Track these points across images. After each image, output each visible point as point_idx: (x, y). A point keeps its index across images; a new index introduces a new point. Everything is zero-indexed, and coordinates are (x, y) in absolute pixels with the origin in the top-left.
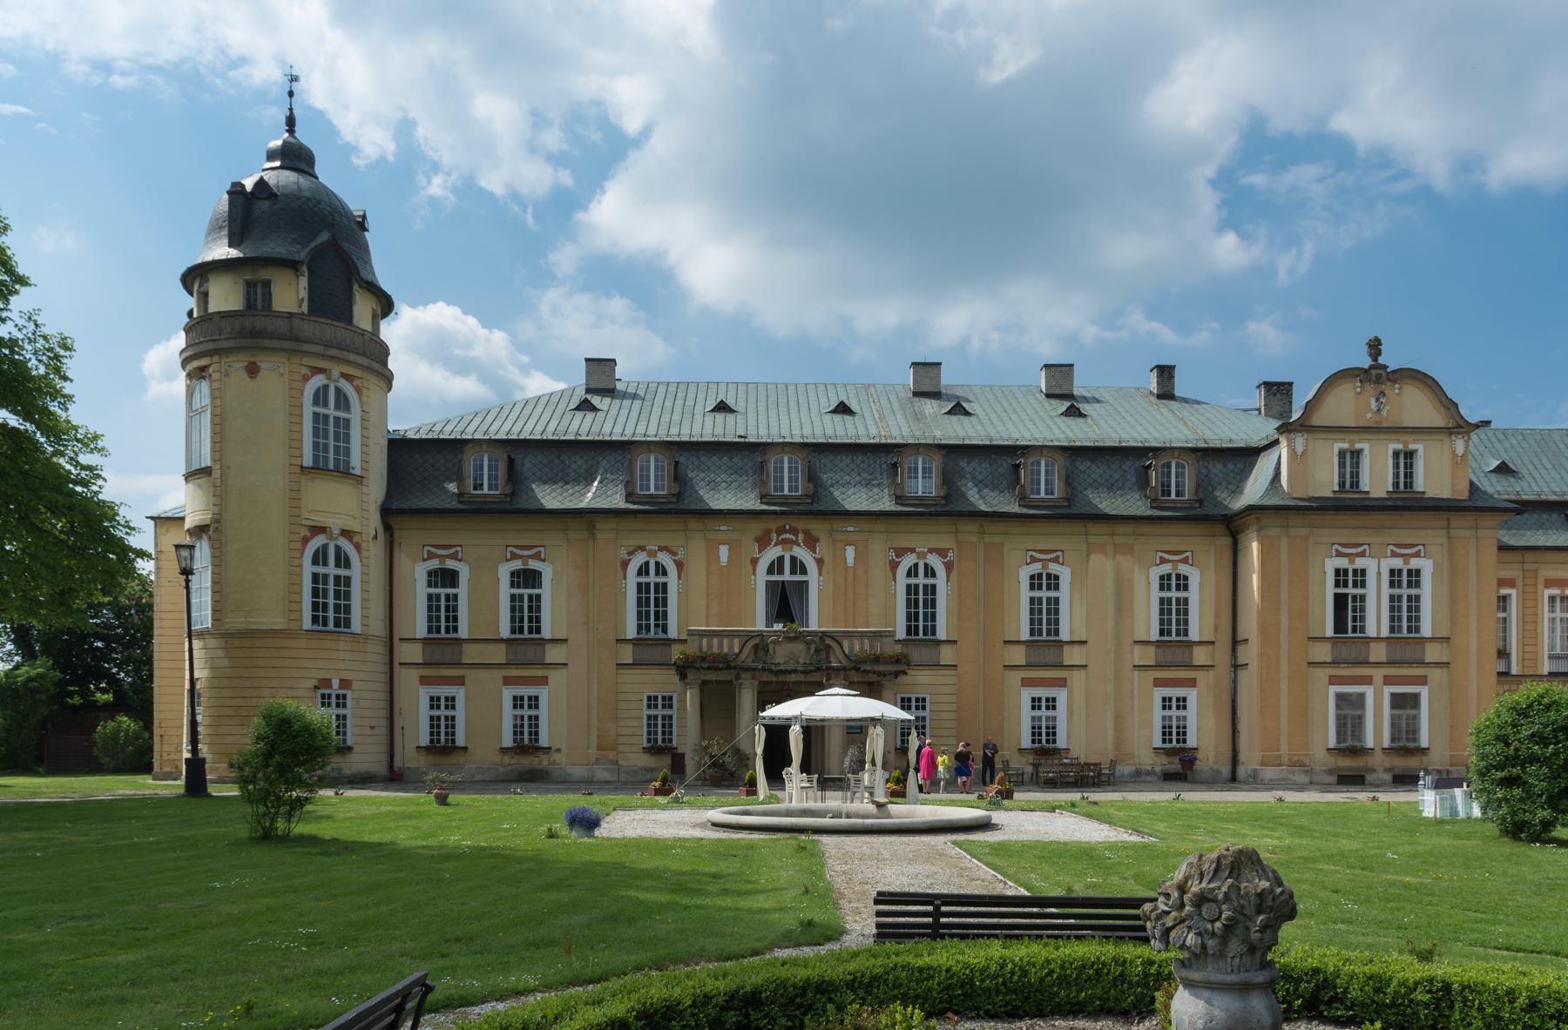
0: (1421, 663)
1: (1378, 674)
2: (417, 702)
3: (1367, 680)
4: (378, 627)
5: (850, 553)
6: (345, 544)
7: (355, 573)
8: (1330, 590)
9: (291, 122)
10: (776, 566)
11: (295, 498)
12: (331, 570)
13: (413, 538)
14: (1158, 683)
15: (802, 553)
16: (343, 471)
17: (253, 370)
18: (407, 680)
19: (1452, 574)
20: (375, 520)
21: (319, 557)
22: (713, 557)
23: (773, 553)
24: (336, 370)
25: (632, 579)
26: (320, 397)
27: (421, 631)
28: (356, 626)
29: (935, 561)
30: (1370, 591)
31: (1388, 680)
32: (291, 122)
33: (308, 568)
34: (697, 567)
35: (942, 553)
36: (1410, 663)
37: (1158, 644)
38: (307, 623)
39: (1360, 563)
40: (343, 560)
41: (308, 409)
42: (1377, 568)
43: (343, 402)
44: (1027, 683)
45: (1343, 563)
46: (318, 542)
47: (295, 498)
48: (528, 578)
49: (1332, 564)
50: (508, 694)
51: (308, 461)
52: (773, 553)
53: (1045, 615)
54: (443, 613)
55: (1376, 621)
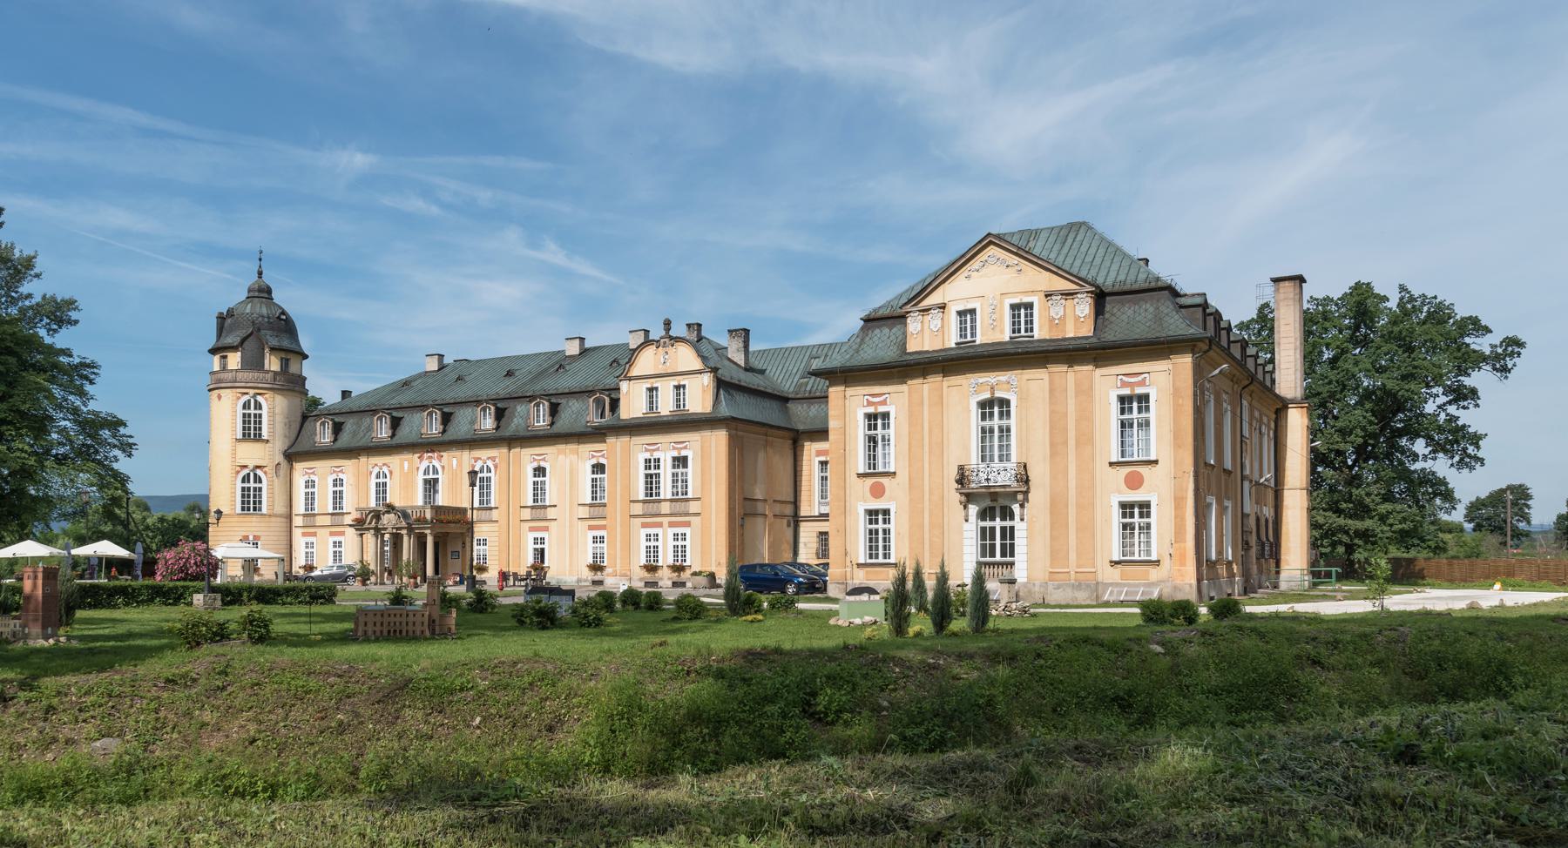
0: (687, 514)
1: (665, 520)
2: (300, 542)
3: (660, 525)
4: (280, 508)
5: (455, 461)
6: (259, 472)
7: (264, 485)
8: (642, 472)
9: (260, 274)
10: (426, 472)
11: (234, 454)
12: (252, 485)
13: (299, 467)
14: (591, 528)
15: (436, 463)
16: (258, 438)
17: (219, 397)
18: (297, 533)
19: (704, 455)
20: (279, 458)
21: (246, 479)
22: (402, 466)
23: (425, 464)
24: (252, 392)
25: (374, 481)
26: (246, 406)
27: (302, 511)
28: (264, 511)
29: (490, 463)
30: (661, 471)
31: (672, 525)
32: (260, 274)
33: (239, 485)
34: (396, 473)
35: (493, 458)
36: (680, 515)
37: (591, 505)
38: (239, 510)
39: (656, 455)
40: (258, 479)
41: (240, 411)
42: (666, 457)
43: (258, 406)
44: (532, 529)
45: (647, 455)
46: (246, 471)
47: (234, 454)
48: (338, 482)
49: (642, 457)
50: (332, 539)
51: (240, 436)
52: (425, 464)
53: (538, 490)
54: (310, 499)
55: (666, 490)
